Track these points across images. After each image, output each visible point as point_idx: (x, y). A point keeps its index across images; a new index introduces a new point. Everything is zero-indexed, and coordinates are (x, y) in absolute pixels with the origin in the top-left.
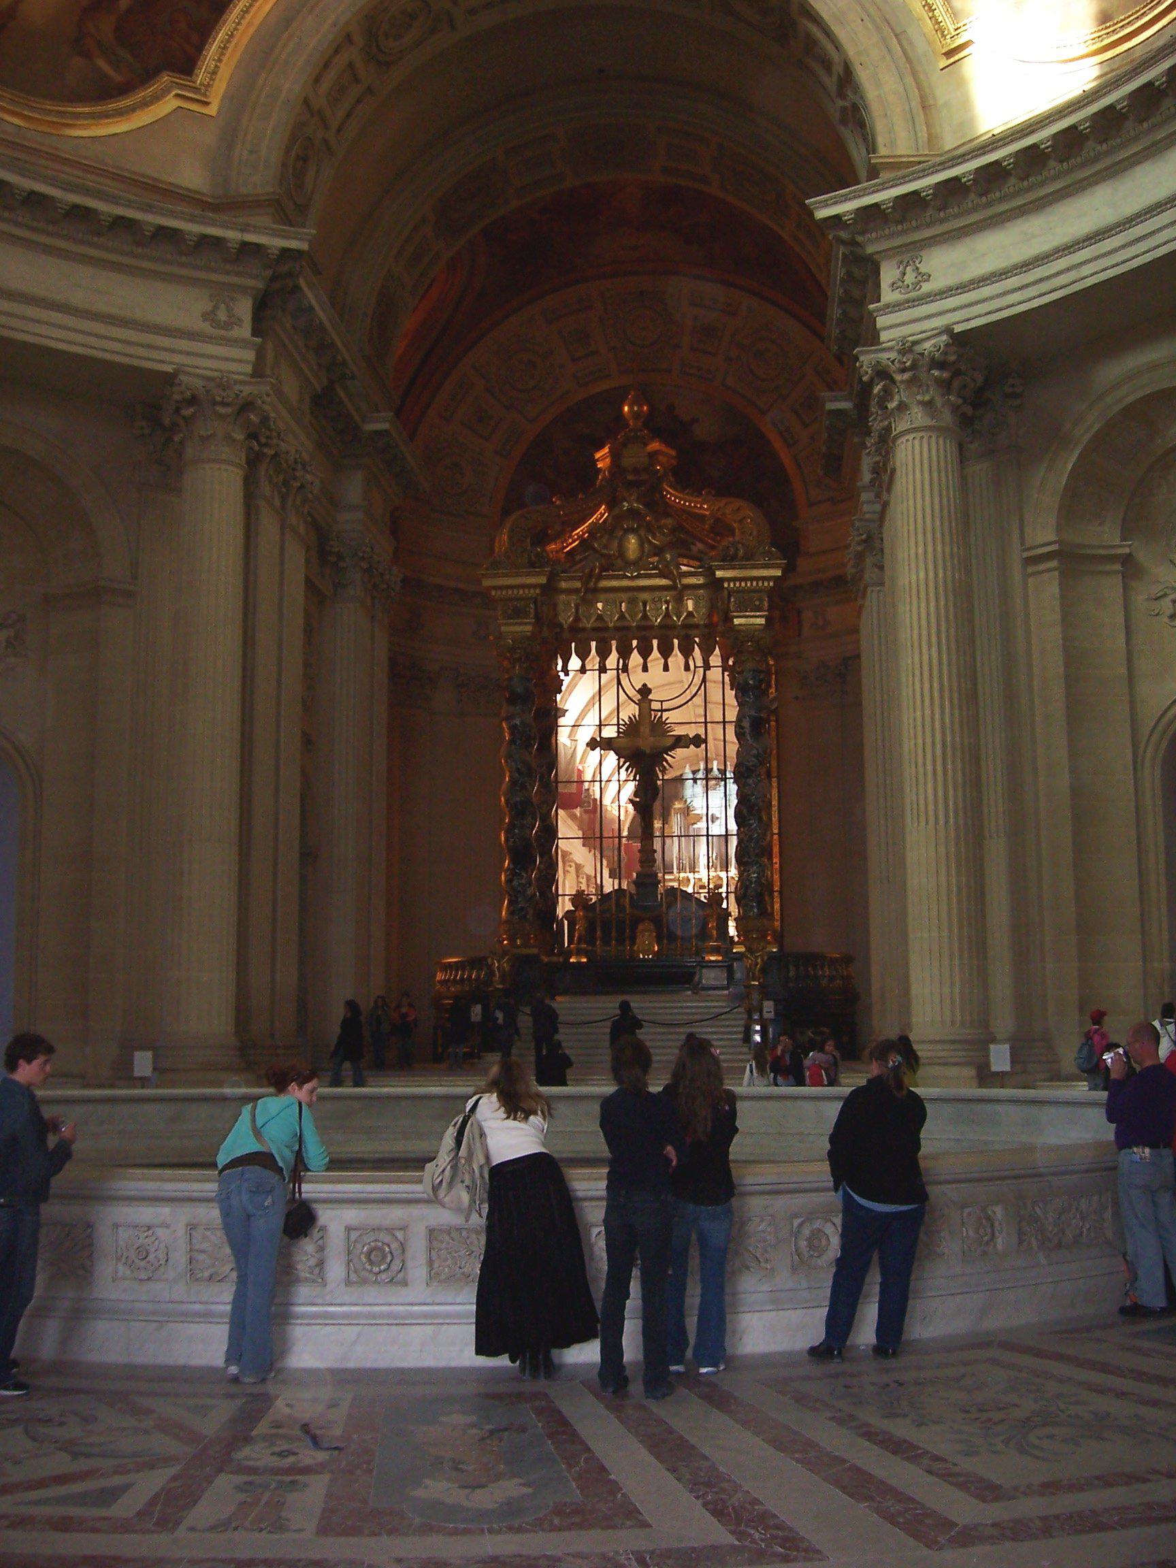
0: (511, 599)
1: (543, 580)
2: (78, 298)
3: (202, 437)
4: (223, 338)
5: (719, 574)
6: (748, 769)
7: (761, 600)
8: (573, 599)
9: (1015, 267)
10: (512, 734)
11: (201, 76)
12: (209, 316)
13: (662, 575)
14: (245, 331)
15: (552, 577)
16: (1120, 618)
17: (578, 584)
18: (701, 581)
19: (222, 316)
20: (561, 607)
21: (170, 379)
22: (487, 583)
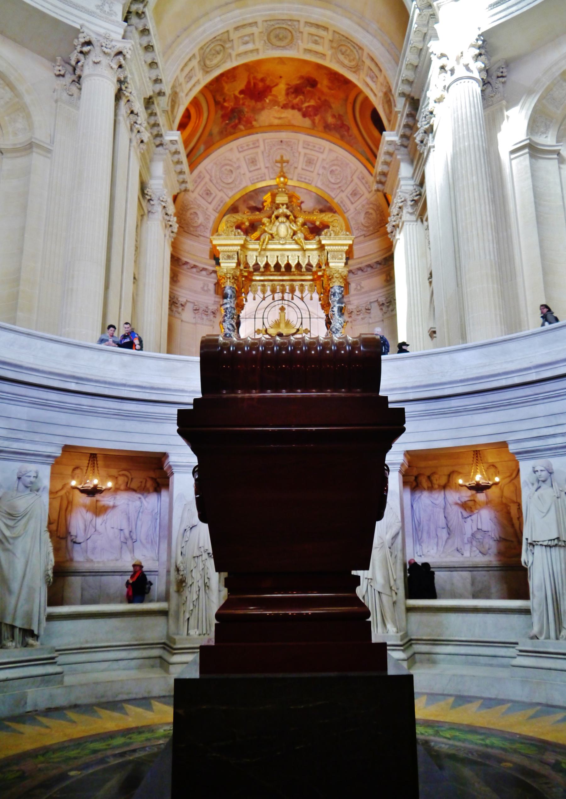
0: (226, 252)
1: (242, 242)
5: (323, 242)
6: (336, 329)
7: (342, 255)
8: (255, 254)
10: (226, 312)
12: (98, 7)
13: (297, 243)
14: (119, 17)
15: (246, 240)
16: (558, 180)
17: (257, 247)
18: (315, 247)
20: (248, 258)
21: (77, 32)
22: (215, 242)
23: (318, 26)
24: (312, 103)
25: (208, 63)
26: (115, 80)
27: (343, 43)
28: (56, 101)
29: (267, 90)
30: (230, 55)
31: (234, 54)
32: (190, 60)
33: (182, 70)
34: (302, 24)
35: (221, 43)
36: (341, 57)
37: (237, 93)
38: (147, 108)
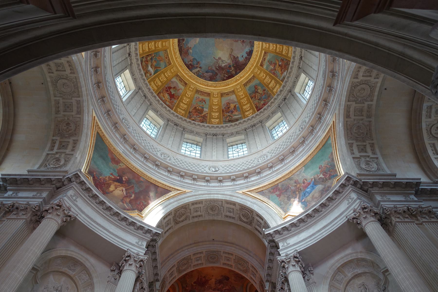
2: (111, 230)
3: (130, 265)
4: (139, 247)
9: (308, 237)
11: (143, 212)
14: (144, 247)
19: (140, 243)
21: (126, 251)
23: (229, 253)
24: (227, 288)
25: (181, 268)
26: (137, 272)
27: (240, 260)
28: (108, 282)
29: (206, 282)
30: (191, 265)
31: (192, 265)
32: (173, 267)
33: (169, 271)
34: (222, 253)
35: (187, 261)
36: (239, 266)
37: (193, 283)
38: (149, 287)
